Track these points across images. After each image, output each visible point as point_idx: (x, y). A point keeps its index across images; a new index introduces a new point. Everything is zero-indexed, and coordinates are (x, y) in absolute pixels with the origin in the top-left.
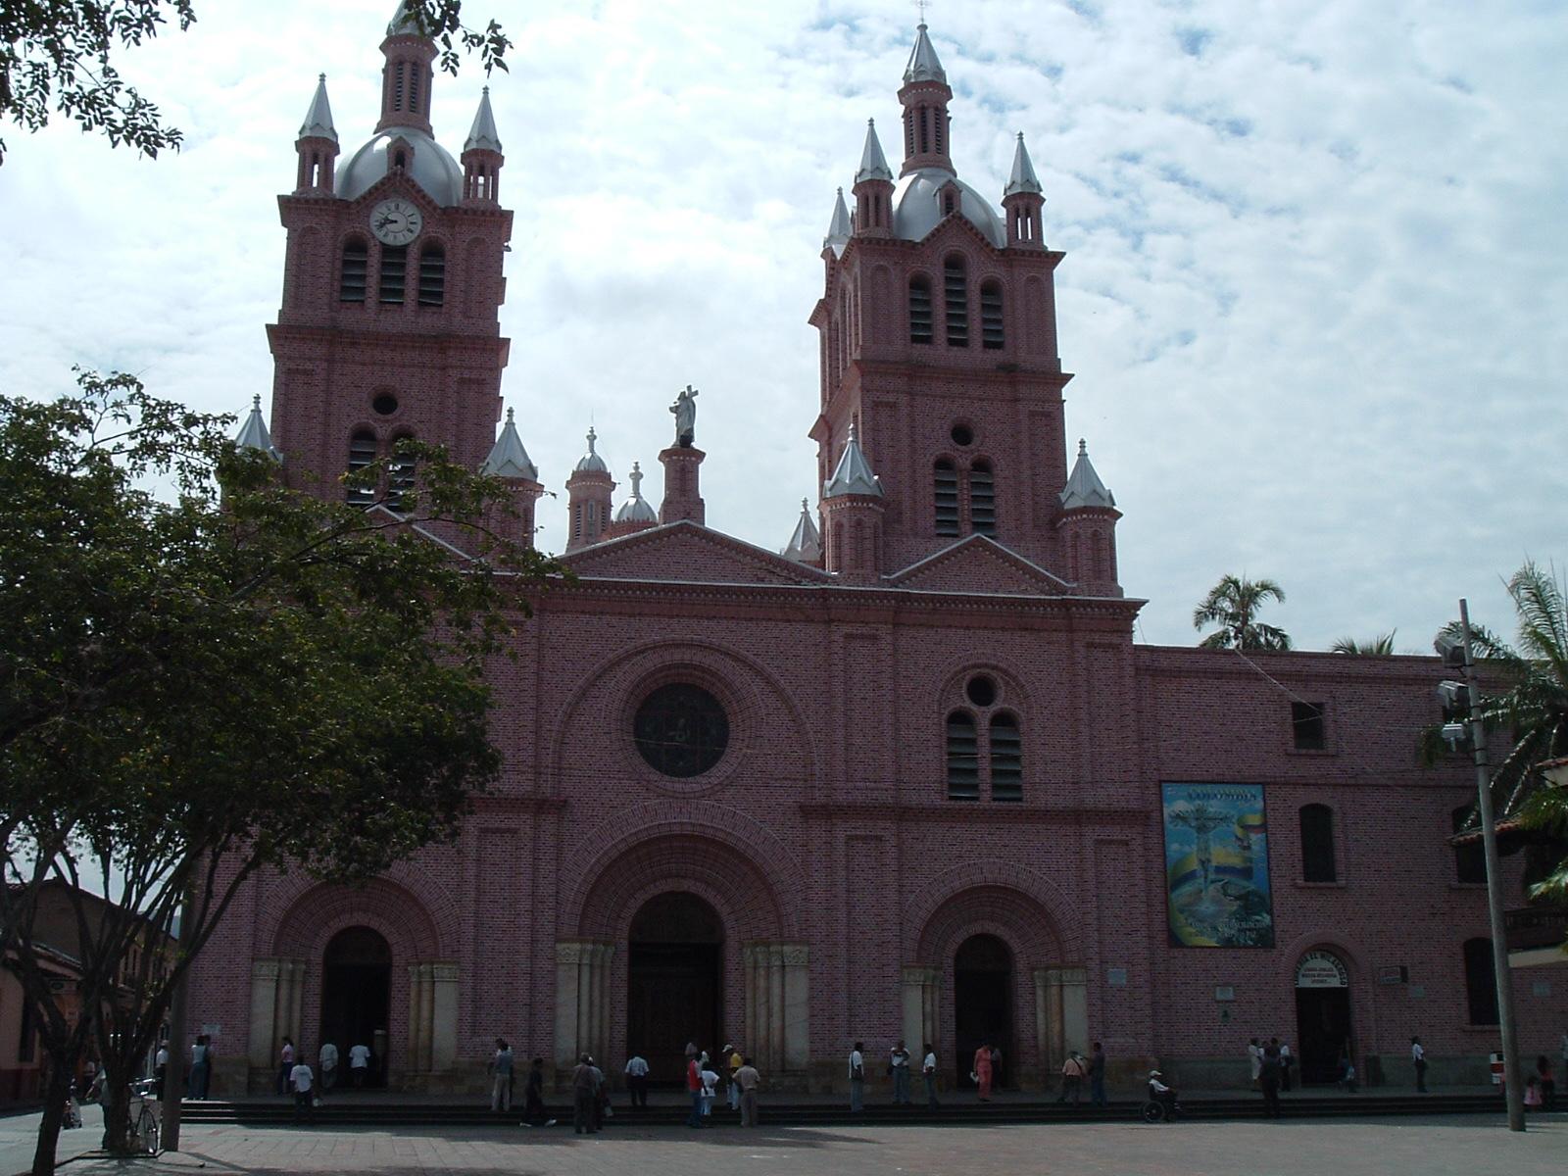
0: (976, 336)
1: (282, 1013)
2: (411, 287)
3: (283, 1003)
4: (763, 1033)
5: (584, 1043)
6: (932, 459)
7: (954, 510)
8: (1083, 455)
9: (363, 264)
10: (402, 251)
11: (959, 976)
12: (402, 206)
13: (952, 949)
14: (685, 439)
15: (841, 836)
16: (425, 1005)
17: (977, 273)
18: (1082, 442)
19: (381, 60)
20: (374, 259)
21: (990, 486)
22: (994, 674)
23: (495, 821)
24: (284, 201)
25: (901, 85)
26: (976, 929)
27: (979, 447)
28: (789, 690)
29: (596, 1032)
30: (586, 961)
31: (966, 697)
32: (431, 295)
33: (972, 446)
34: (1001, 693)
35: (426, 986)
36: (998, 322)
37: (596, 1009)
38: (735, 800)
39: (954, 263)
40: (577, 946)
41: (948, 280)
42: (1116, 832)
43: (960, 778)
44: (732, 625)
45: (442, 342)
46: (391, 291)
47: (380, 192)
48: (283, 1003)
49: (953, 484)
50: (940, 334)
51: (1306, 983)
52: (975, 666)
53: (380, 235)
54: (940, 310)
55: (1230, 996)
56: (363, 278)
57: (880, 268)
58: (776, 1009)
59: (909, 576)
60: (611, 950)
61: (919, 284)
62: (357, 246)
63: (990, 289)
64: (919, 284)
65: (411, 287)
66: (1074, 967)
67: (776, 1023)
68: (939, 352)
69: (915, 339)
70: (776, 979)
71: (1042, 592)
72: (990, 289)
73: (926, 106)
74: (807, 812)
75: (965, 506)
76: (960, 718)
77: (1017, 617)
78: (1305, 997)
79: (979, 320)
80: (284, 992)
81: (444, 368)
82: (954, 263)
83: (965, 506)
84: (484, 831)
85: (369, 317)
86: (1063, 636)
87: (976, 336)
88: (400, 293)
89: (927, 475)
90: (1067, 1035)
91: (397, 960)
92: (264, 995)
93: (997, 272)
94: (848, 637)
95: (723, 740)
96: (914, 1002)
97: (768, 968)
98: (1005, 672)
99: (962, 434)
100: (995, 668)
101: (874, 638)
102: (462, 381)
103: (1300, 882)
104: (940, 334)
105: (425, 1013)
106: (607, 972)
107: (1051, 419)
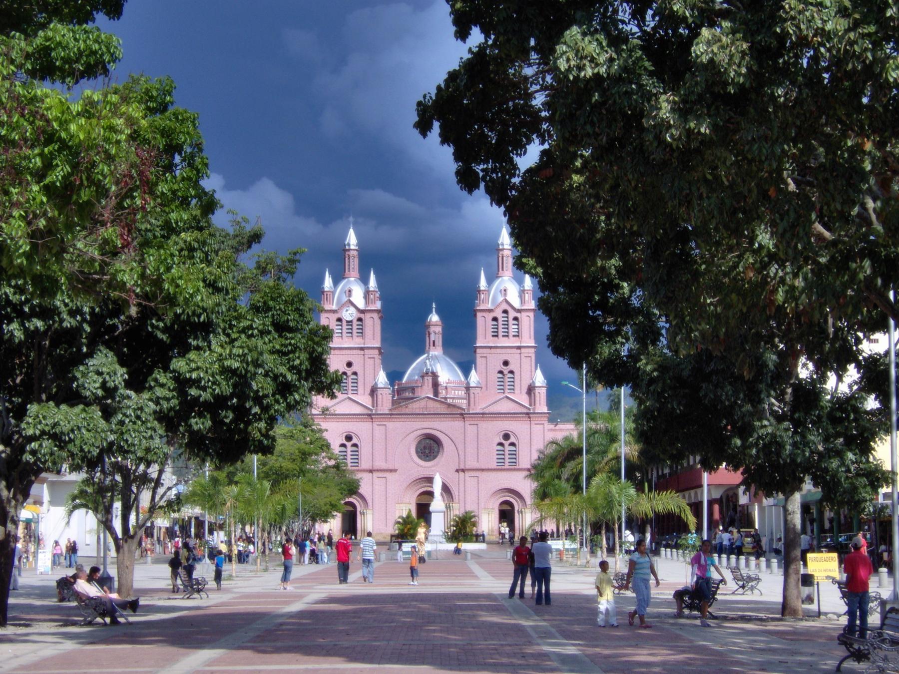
10: (351, 321)
17: (512, 314)
20: (344, 323)
27: (511, 367)
32: (361, 333)
62: (339, 320)
63: (516, 319)
74: (457, 471)
76: (501, 444)
93: (518, 315)
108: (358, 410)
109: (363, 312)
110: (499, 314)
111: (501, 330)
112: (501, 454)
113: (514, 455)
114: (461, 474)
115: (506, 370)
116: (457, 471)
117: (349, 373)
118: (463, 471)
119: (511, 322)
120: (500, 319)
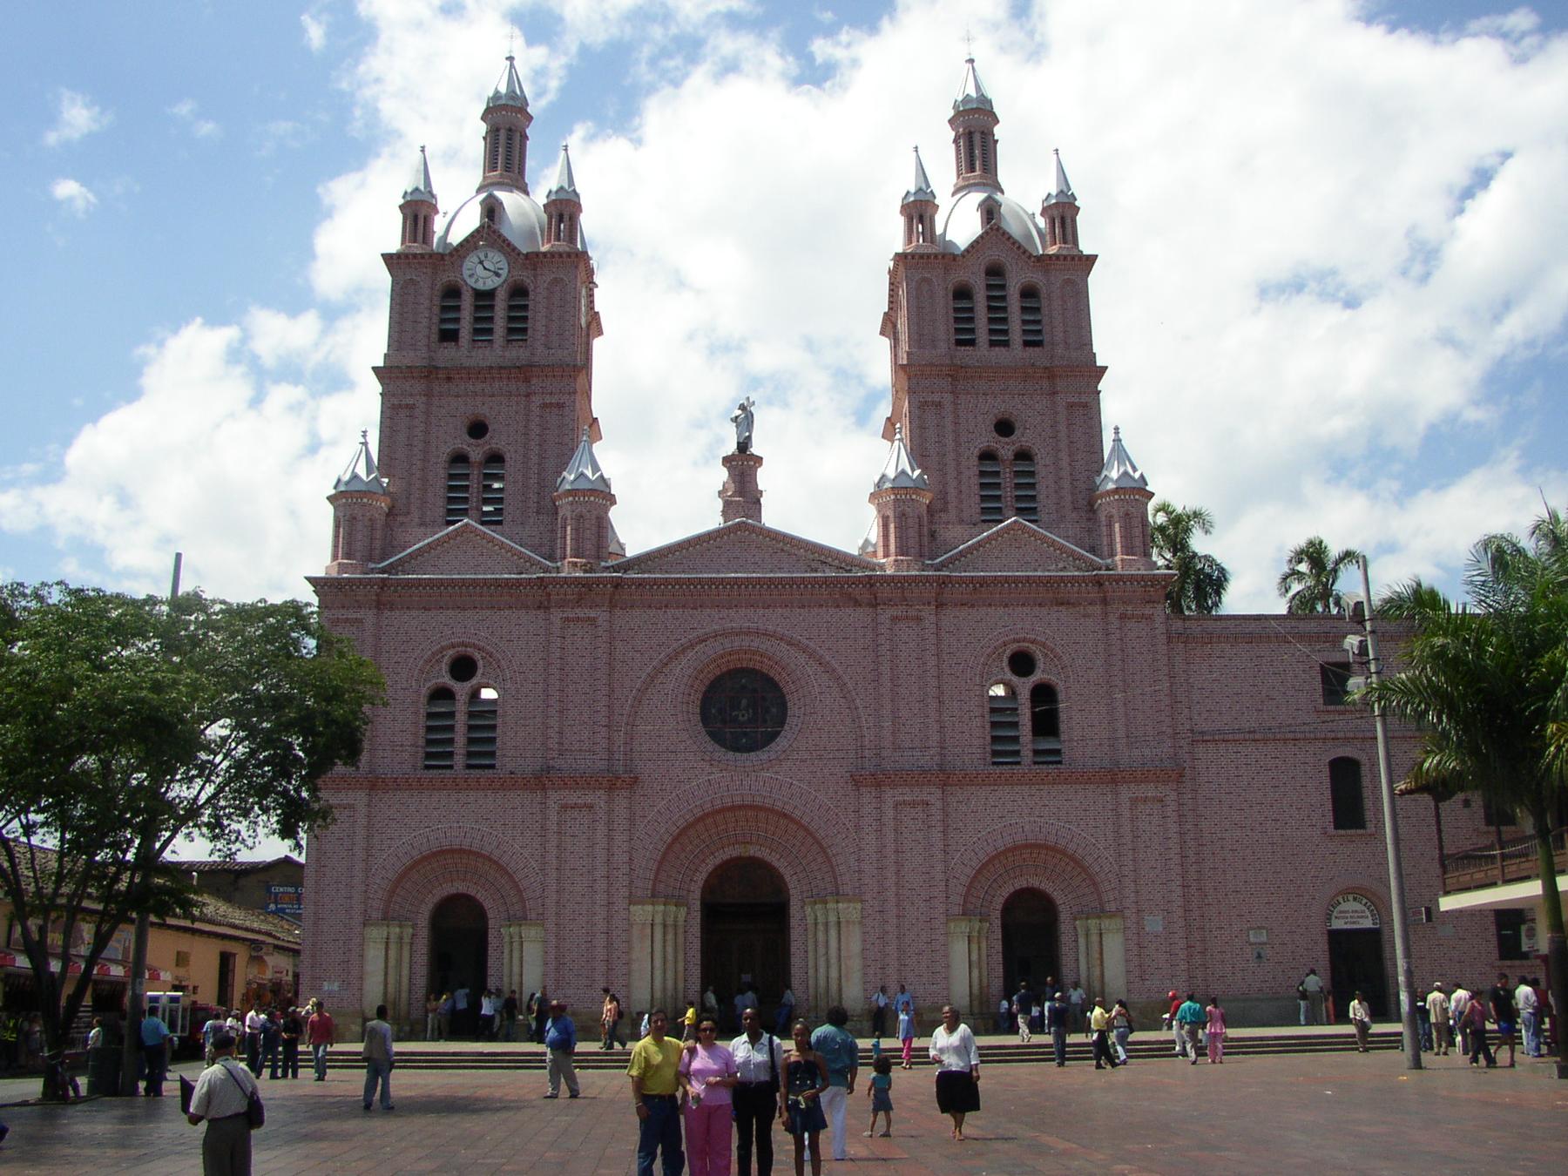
0: (1016, 336)
1: (391, 972)
2: (500, 325)
3: (392, 962)
4: (822, 982)
5: (658, 994)
6: (976, 452)
7: (998, 498)
8: (1117, 441)
9: (457, 308)
10: (490, 294)
12: (490, 255)
13: (999, 903)
14: (743, 446)
15: (890, 802)
16: (516, 961)
18: (1117, 429)
19: (483, 128)
20: (467, 302)
21: (1032, 474)
22: (1033, 647)
23: (573, 797)
24: (388, 259)
25: (952, 113)
26: (1021, 883)
28: (840, 671)
29: (670, 983)
30: (659, 919)
31: (1007, 669)
32: (518, 328)
33: (1013, 437)
34: (1040, 664)
35: (516, 945)
36: (1038, 322)
37: (670, 965)
38: (790, 774)
39: (995, 271)
40: (649, 908)
41: (989, 287)
42: (1150, 791)
44: (786, 612)
45: (524, 372)
46: (482, 330)
47: (470, 242)
48: (392, 962)
49: (997, 474)
50: (982, 336)
51: (1338, 924)
52: (1015, 640)
53: (471, 282)
55: (1264, 939)
56: (457, 320)
57: (924, 279)
58: (833, 961)
59: (952, 560)
60: (683, 910)
61: (962, 293)
62: (453, 292)
63: (1029, 293)
65: (500, 325)
66: (1112, 915)
67: (834, 974)
68: (982, 352)
69: (959, 343)
70: (833, 933)
71: (1079, 569)
72: (1029, 293)
73: (976, 133)
75: (1008, 492)
77: (1053, 593)
78: (1335, 937)
79: (985, 320)
80: (392, 953)
81: (528, 395)
82: (995, 271)
83: (1008, 492)
84: (565, 807)
85: (463, 353)
86: (1098, 609)
87: (1016, 336)
88: (490, 331)
89: (972, 466)
90: (1106, 979)
91: (491, 923)
92: (374, 957)
94: (894, 619)
95: (781, 721)
96: (959, 951)
97: (826, 924)
98: (1044, 645)
99: (1004, 427)
100: (1033, 642)
101: (919, 619)
102: (544, 406)
103: (1331, 830)
104: (982, 336)
105: (516, 969)
106: (681, 931)
107: (1087, 410)
113: (1046, 723)
114: (868, 796)
117: (476, 452)
119: (1014, 303)
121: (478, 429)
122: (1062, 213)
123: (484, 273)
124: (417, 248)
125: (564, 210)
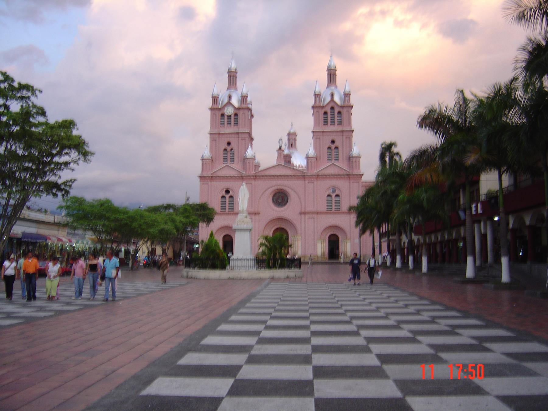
0: (336, 123)
10: (231, 116)
11: (329, 241)
14: (280, 148)
17: (336, 111)
20: (226, 117)
27: (337, 144)
32: (236, 123)
39: (332, 108)
43: (329, 206)
46: (229, 123)
54: (329, 119)
61: (325, 113)
62: (223, 115)
63: (339, 113)
64: (325, 113)
73: (332, 75)
74: (301, 213)
82: (332, 108)
89: (326, 150)
93: (341, 110)
99: (333, 142)
107: (350, 138)
108: (234, 173)
109: (238, 109)
110: (328, 110)
111: (329, 121)
112: (329, 202)
113: (338, 203)
114: (303, 216)
115: (333, 147)
116: (301, 213)
118: (305, 213)
120: (329, 114)
121: (229, 144)
122: (347, 95)
123: (229, 111)
124: (215, 106)
125: (244, 98)
